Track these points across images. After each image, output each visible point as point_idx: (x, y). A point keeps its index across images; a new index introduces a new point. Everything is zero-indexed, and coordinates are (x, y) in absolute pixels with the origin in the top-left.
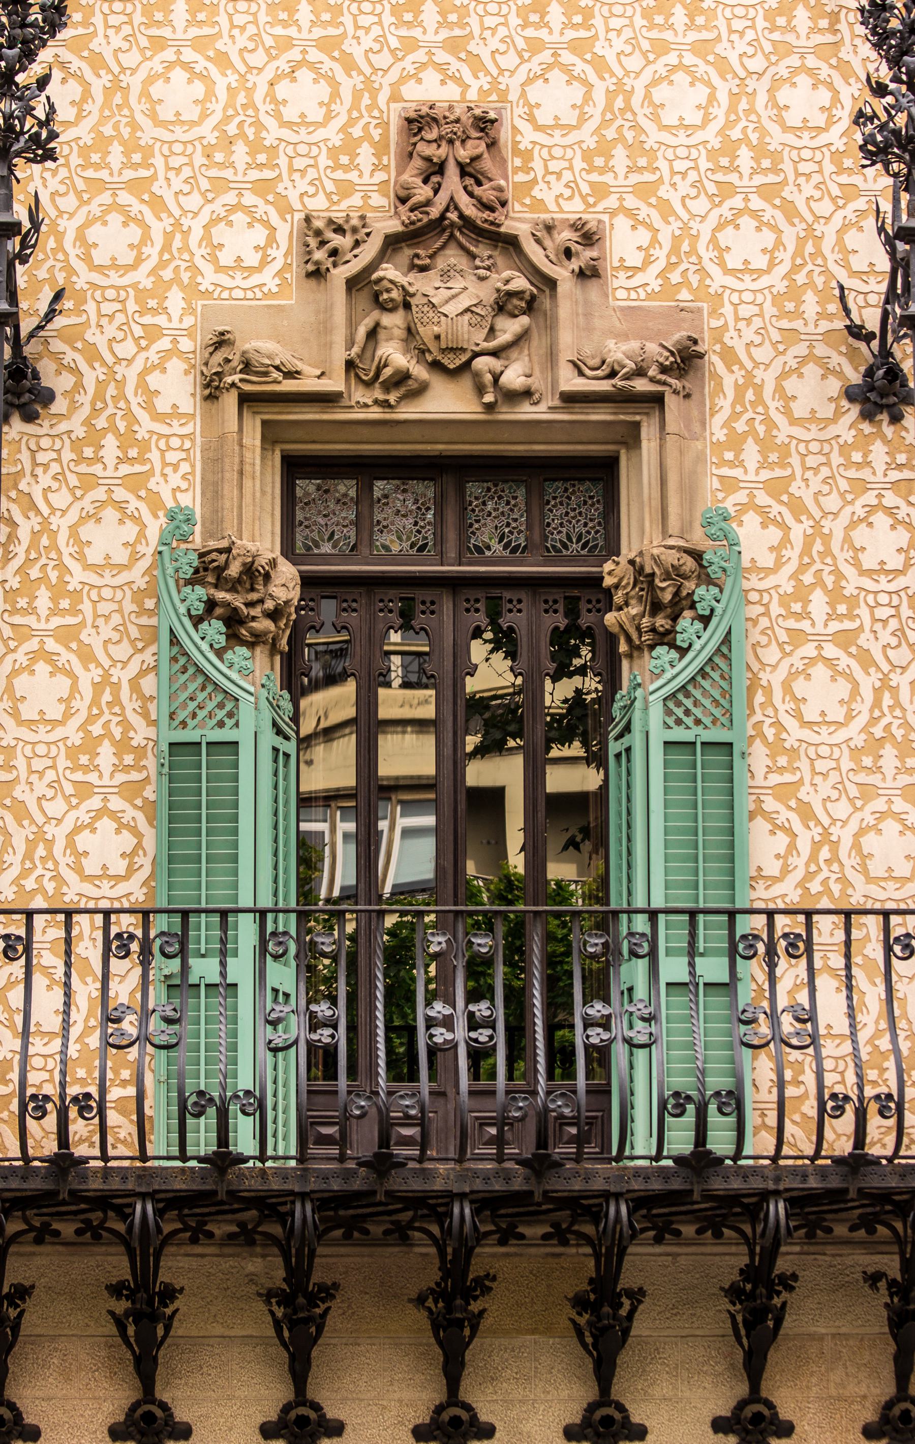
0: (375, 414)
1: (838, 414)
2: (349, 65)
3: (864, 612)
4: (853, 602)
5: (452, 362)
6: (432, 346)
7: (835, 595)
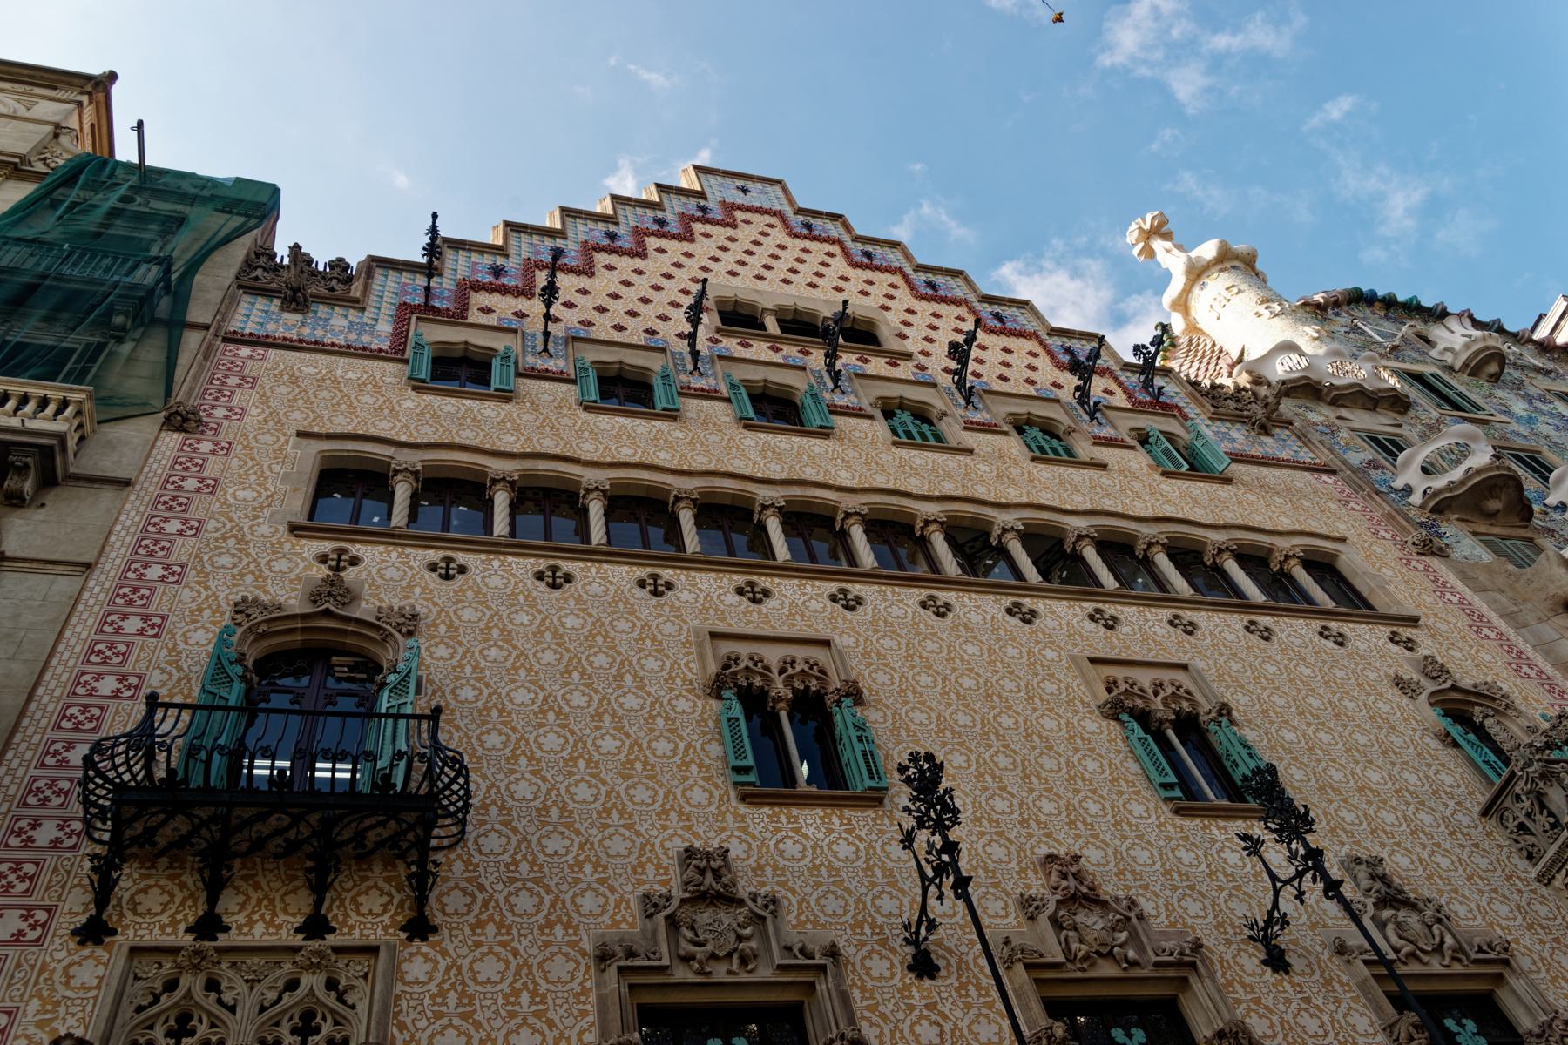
0: (1079, 975)
1: (1263, 973)
5: (1105, 950)
6: (1093, 943)
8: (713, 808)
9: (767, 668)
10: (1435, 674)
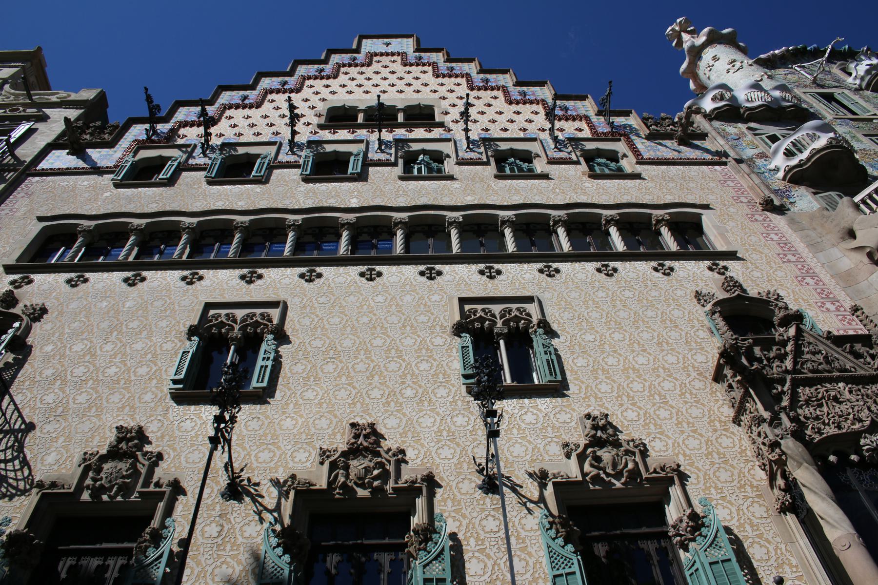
2: (335, 416)
3: (487, 543)
4: (483, 540)
7: (477, 539)
8: (152, 405)
9: (235, 321)
10: (729, 288)
